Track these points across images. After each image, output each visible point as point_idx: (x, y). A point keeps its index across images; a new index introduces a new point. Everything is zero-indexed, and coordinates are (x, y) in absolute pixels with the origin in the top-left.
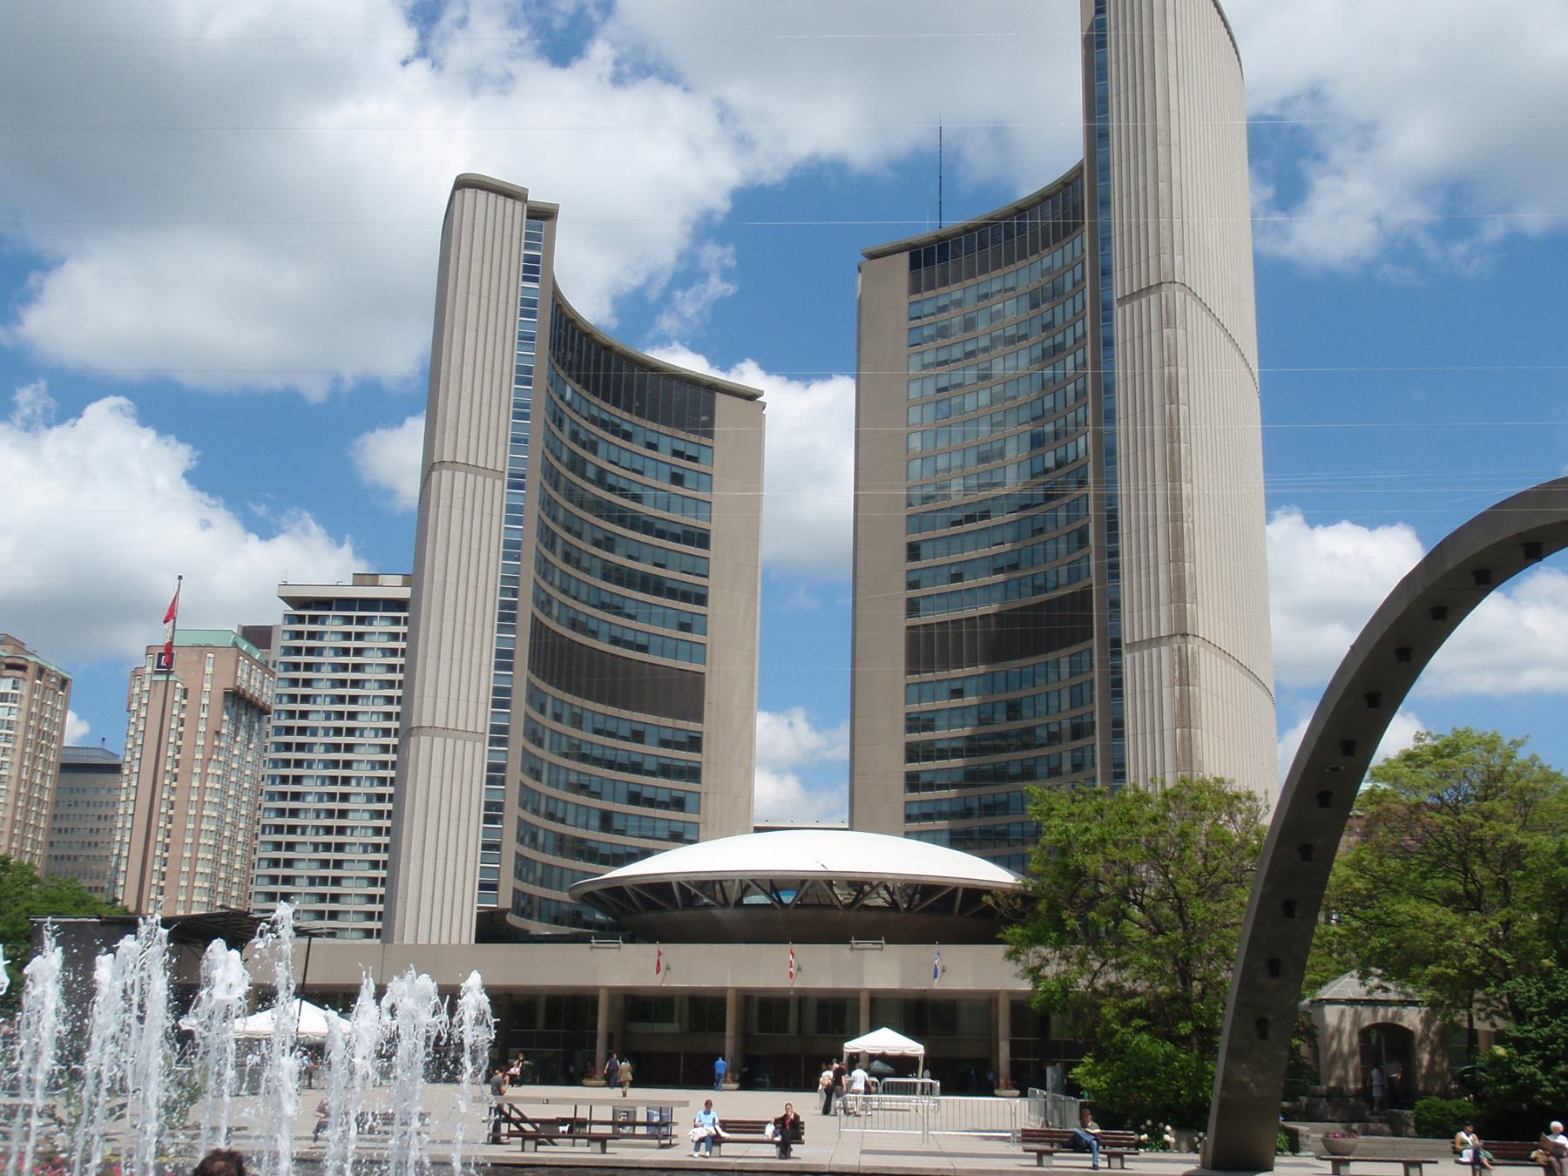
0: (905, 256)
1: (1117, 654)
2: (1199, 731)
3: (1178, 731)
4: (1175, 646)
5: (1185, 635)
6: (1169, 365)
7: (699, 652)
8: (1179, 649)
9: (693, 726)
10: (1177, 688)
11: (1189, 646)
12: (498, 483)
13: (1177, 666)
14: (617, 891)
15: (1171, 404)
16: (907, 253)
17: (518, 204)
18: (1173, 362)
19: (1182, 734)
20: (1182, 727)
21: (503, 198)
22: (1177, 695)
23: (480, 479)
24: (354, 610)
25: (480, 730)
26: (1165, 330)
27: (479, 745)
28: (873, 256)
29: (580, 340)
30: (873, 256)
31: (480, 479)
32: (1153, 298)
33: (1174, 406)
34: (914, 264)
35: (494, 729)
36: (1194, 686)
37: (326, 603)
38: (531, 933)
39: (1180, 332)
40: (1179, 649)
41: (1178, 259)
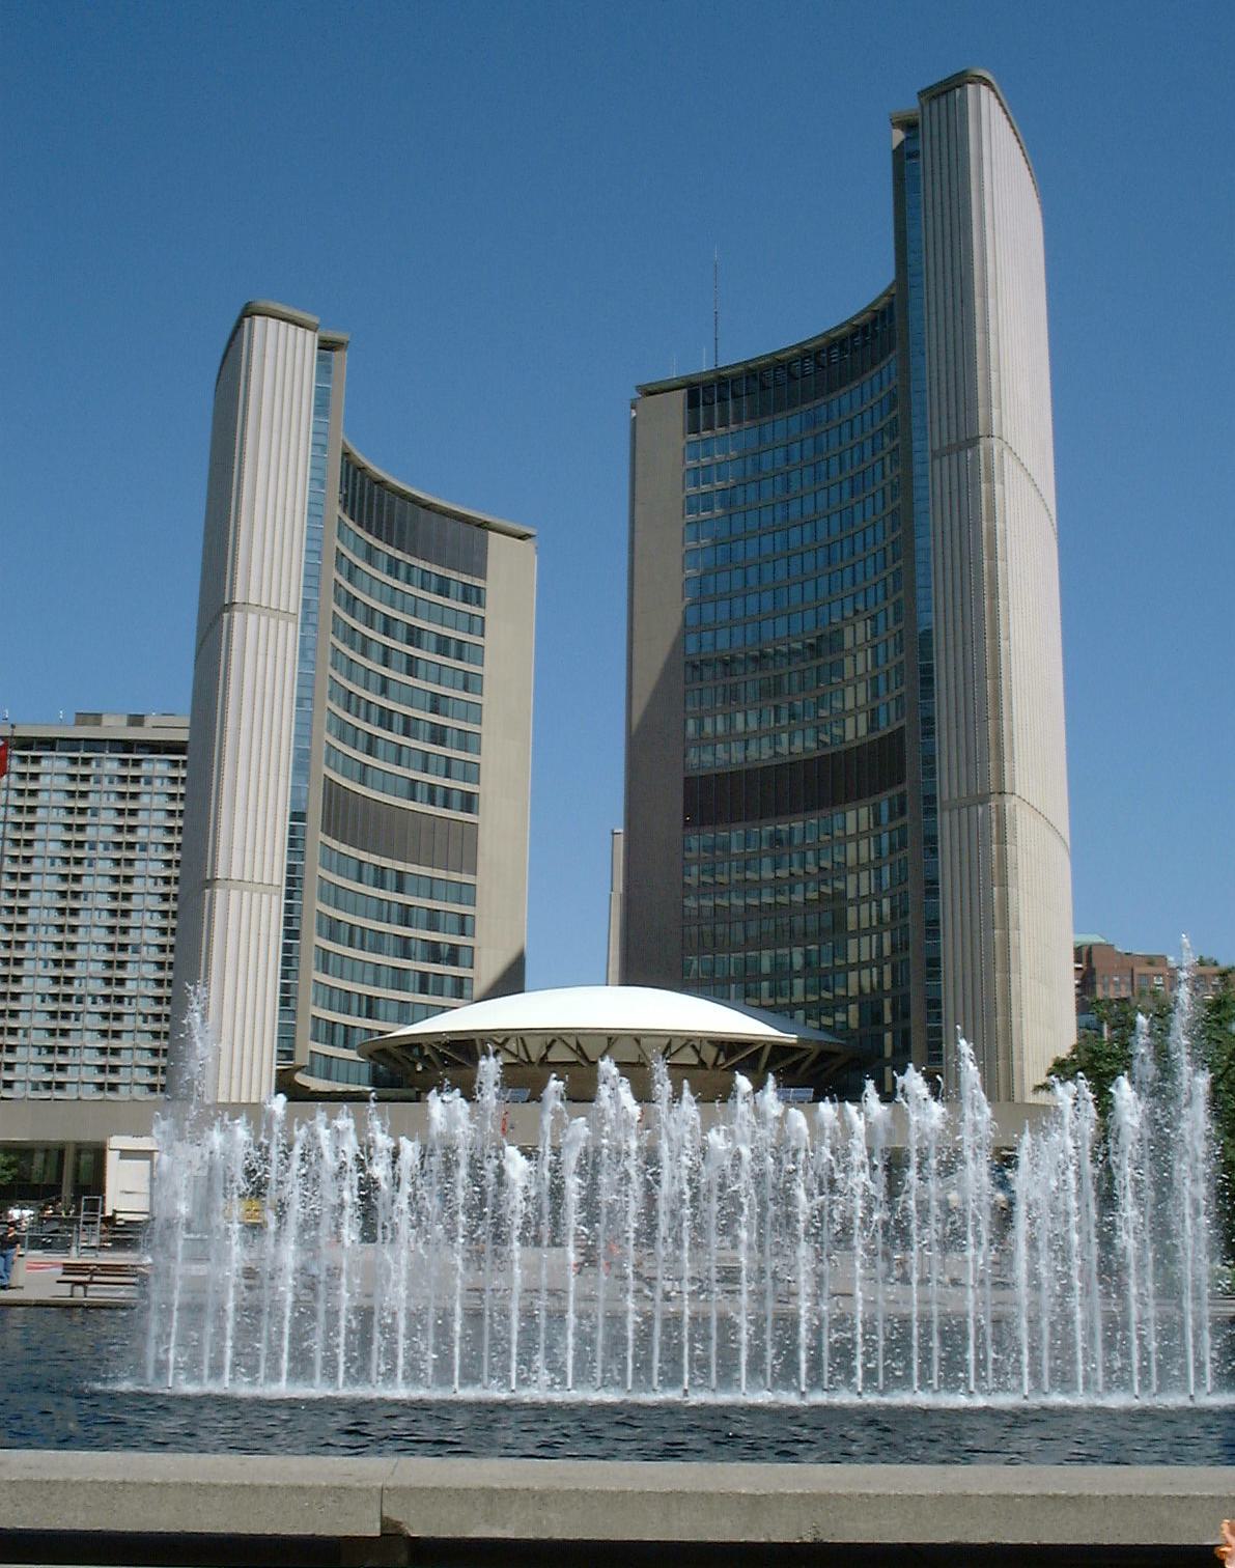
0: (680, 396)
1: (931, 811)
2: (1015, 890)
5: (1001, 793)
7: (469, 802)
9: (465, 878)
12: (291, 626)
14: (412, 1046)
16: (685, 391)
17: (310, 333)
21: (293, 327)
23: (273, 622)
24: (78, 750)
25: (276, 882)
27: (275, 899)
28: (650, 393)
29: (355, 474)
30: (650, 393)
31: (273, 622)
34: (692, 403)
35: (290, 882)
37: (49, 744)
38: (312, 1089)
41: (995, 412)
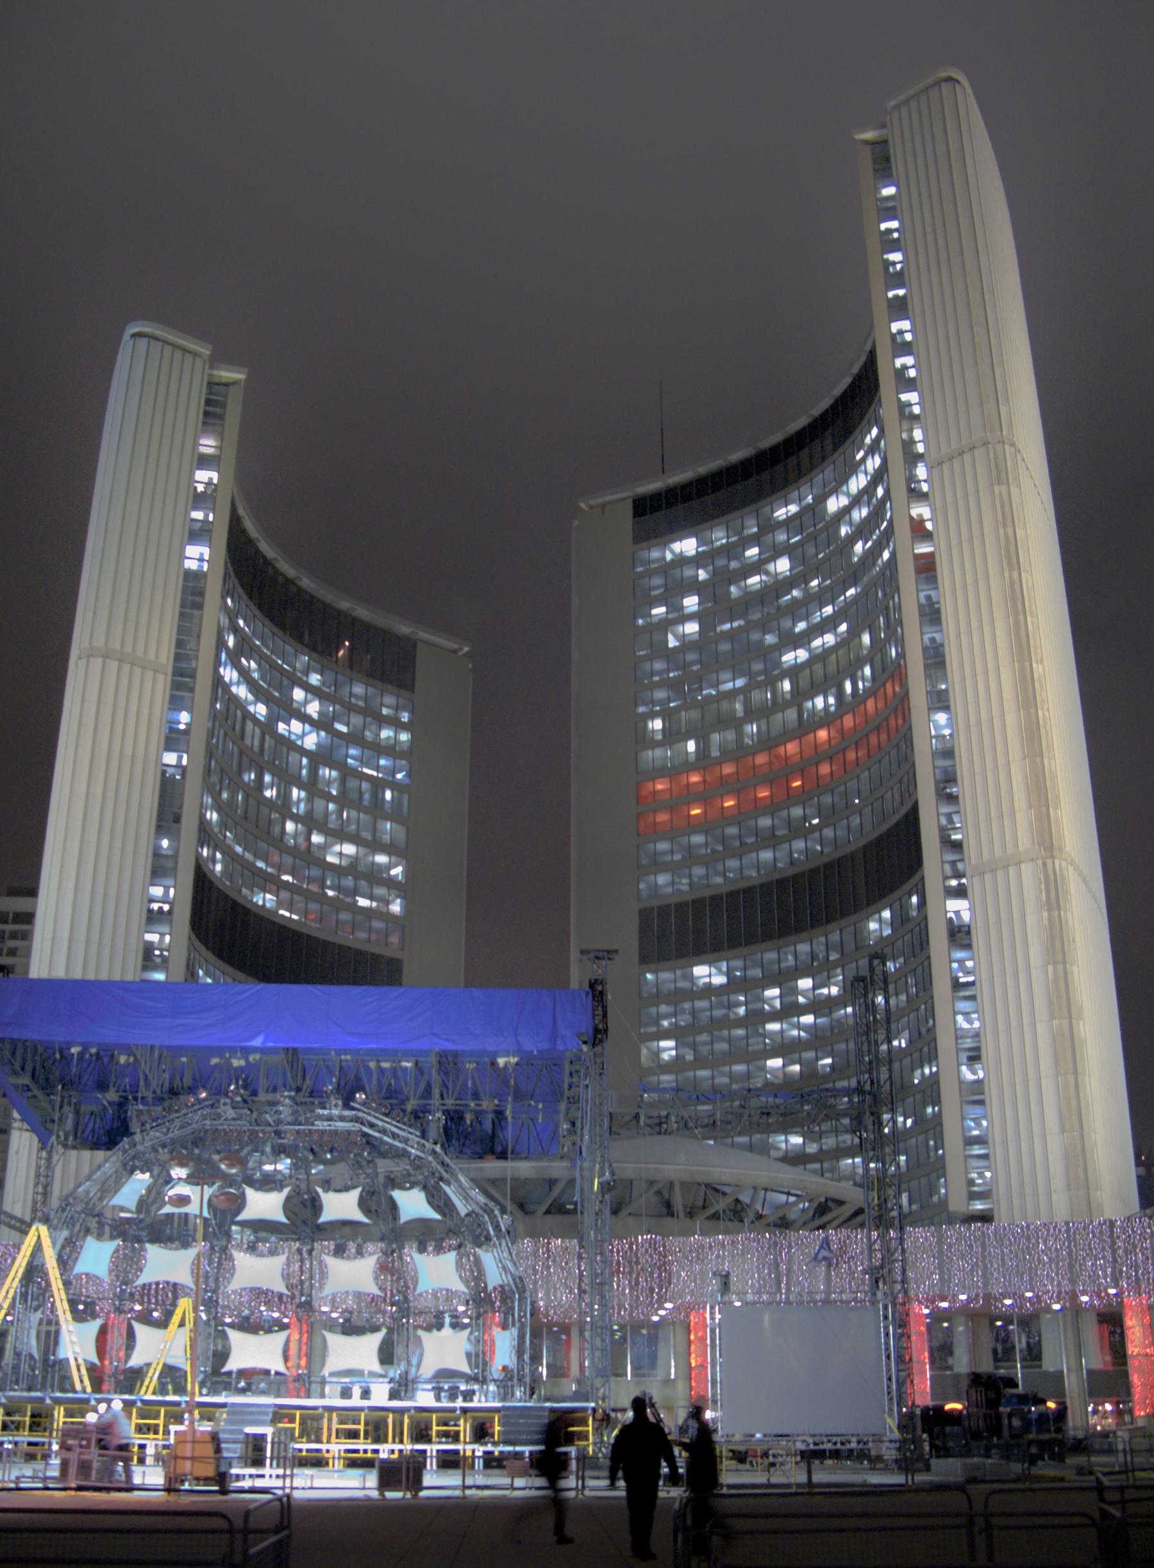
3: (1050, 968)
4: (1040, 862)
6: (1005, 526)
8: (1044, 865)
10: (1045, 914)
11: (1057, 862)
13: (1043, 887)
15: (1011, 569)
18: (1009, 522)
19: (1055, 971)
20: (1055, 963)
22: (1046, 921)
26: (996, 488)
32: (979, 453)
33: (1015, 574)
36: (1065, 911)
39: (1013, 490)
40: (1044, 865)
